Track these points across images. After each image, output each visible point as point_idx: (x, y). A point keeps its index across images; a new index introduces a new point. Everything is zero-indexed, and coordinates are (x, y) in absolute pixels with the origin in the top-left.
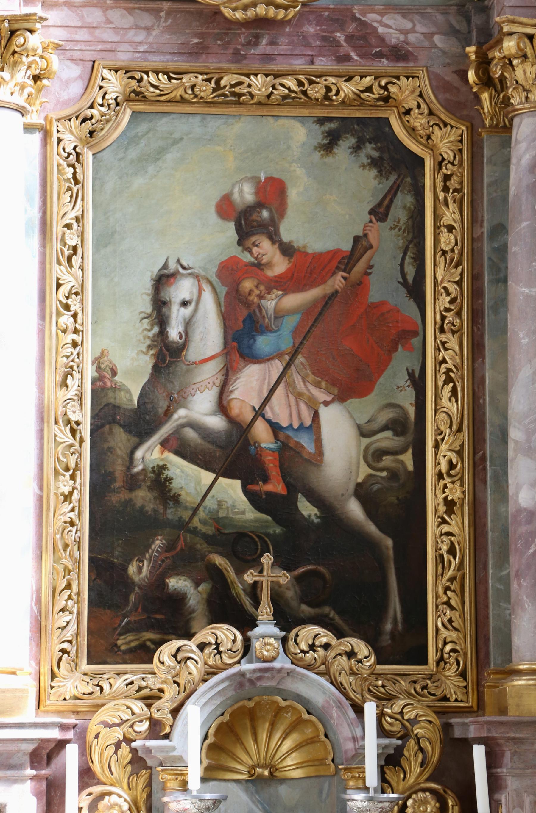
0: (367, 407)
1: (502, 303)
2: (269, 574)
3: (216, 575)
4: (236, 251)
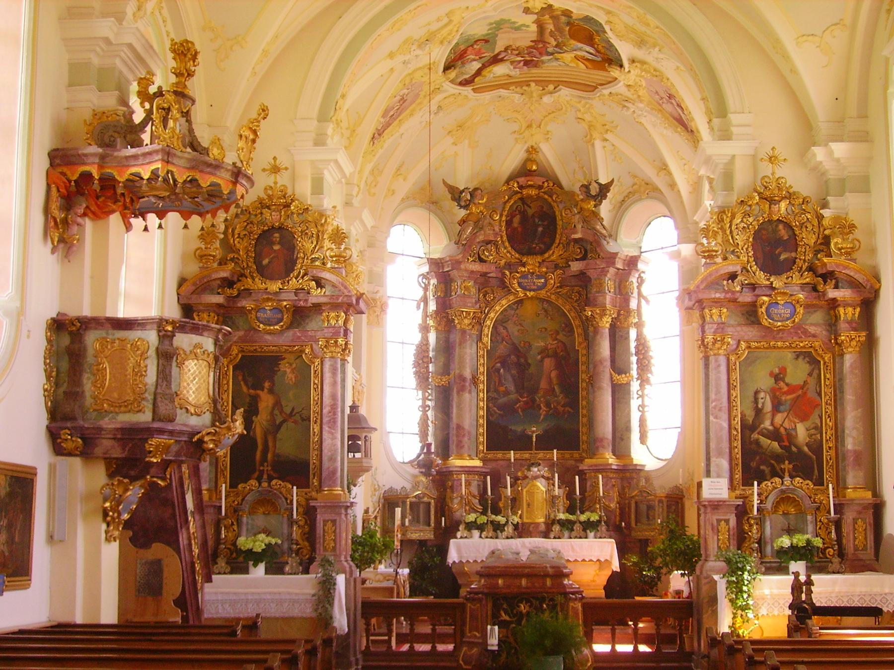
0: (808, 423)
1: (842, 398)
2: (787, 466)
3: (772, 466)
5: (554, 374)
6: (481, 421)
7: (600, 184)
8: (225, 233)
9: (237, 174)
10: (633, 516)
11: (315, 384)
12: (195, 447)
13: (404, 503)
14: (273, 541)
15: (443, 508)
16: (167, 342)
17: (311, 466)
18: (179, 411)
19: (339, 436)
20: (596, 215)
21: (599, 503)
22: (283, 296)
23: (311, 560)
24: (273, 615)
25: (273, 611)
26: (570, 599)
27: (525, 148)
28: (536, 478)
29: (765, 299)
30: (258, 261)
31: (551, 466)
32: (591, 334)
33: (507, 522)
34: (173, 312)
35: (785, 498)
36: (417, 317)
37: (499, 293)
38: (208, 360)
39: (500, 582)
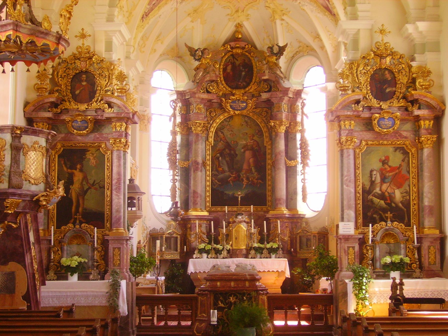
0: (402, 190)
1: (422, 175)
2: (389, 215)
3: (380, 215)
4: (382, 167)
5: (251, 160)
6: (208, 188)
7: (279, 47)
8: (53, 74)
9: (59, 38)
10: (298, 245)
11: (107, 166)
12: (34, 204)
13: (162, 237)
14: (83, 260)
15: (185, 240)
16: (17, 140)
17: (106, 216)
18: (24, 182)
19: (122, 197)
20: (277, 65)
21: (278, 237)
22: (88, 113)
23: (106, 272)
24: (82, 305)
25: (83, 302)
26: (260, 293)
27: (235, 24)
28: (240, 222)
29: (377, 115)
30: (73, 92)
31: (250, 215)
32: (274, 137)
33: (223, 248)
34: (21, 122)
35: (388, 234)
36: (169, 126)
37: (219, 112)
38: (42, 151)
39: (218, 284)
